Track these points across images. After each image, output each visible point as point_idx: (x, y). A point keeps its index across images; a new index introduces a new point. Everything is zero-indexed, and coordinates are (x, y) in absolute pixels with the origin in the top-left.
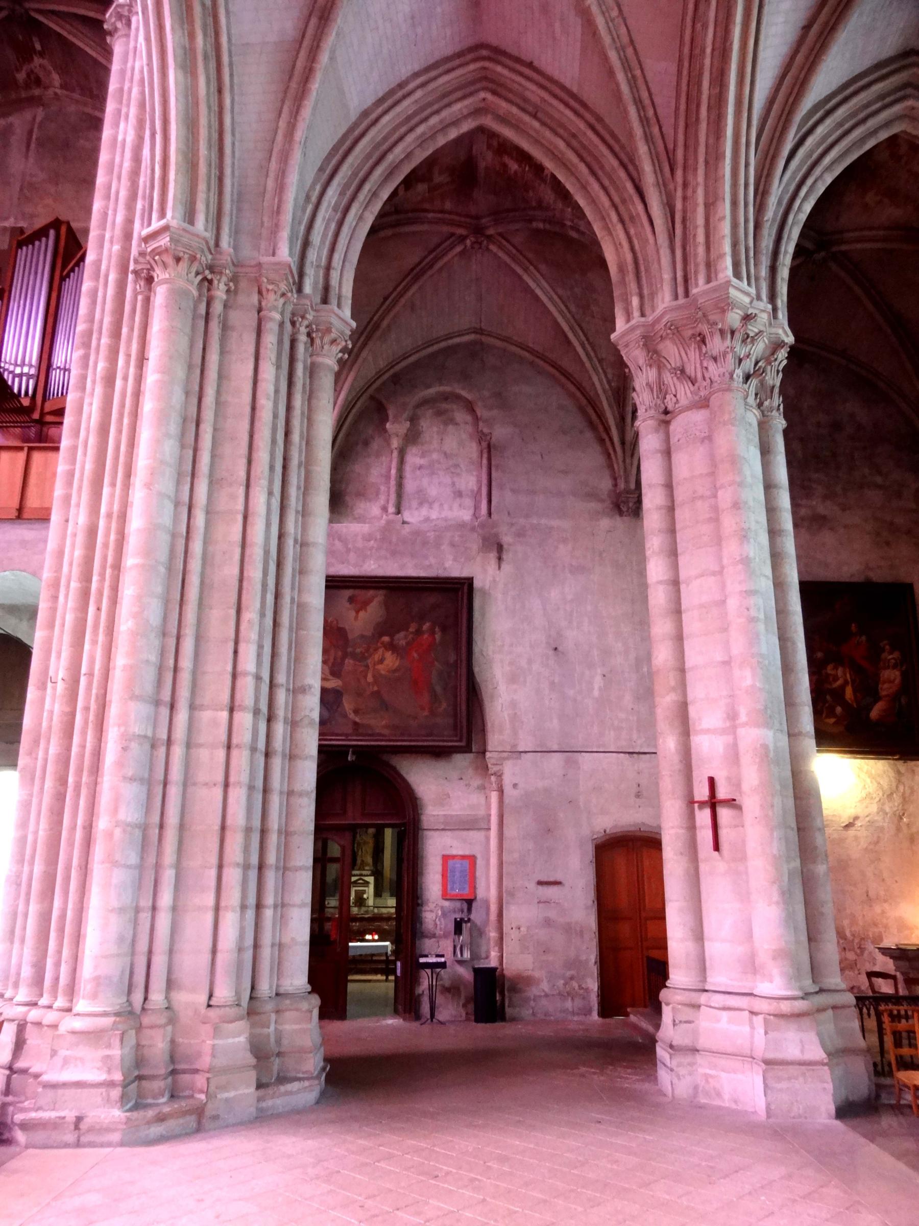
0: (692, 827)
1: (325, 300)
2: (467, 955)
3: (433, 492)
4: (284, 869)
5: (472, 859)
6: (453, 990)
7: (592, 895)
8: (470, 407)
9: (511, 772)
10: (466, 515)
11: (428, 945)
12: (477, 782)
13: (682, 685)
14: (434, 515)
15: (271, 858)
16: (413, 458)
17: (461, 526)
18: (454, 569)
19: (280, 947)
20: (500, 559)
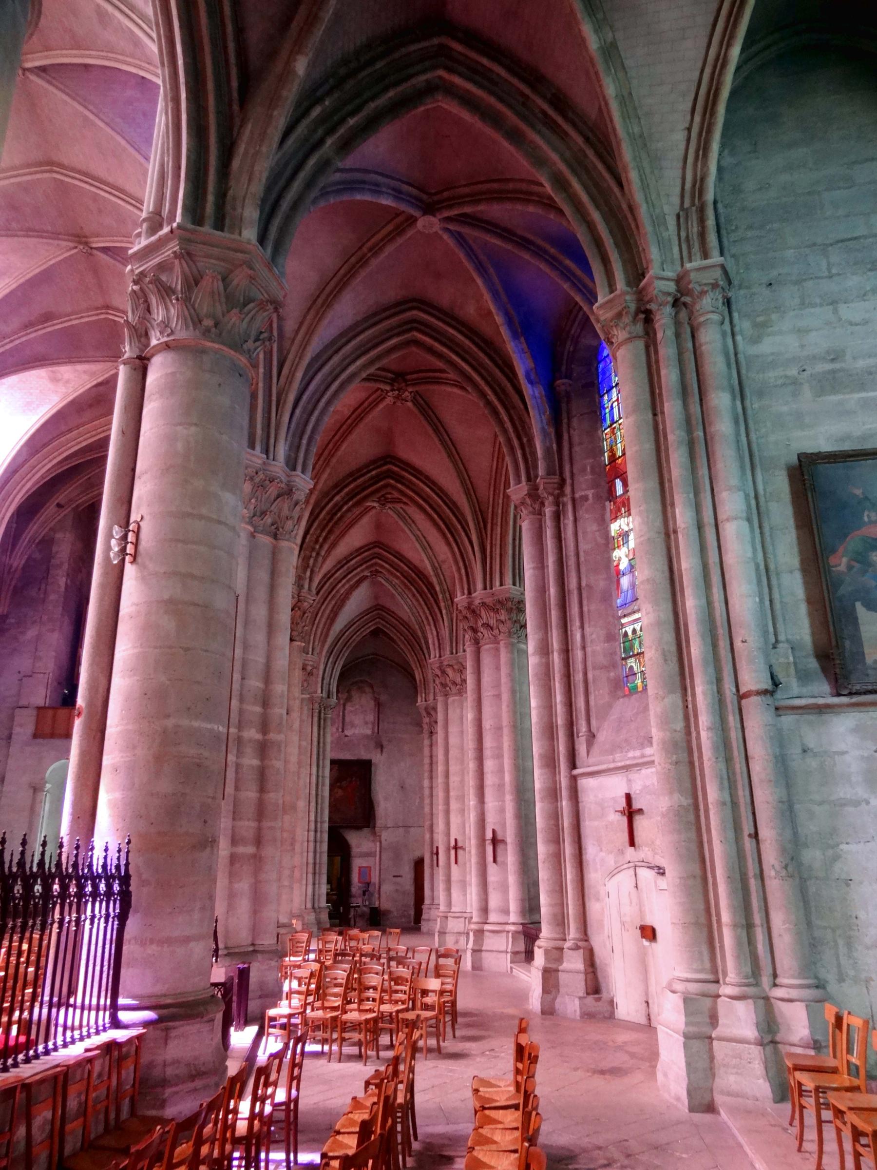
0: (432, 860)
1: (329, 697)
2: (367, 903)
3: (356, 722)
4: (320, 874)
5: (370, 867)
6: (362, 916)
7: (412, 881)
8: (372, 686)
9: (385, 835)
10: (369, 732)
11: (353, 900)
12: (372, 838)
13: (432, 819)
14: (357, 732)
15: (317, 871)
16: (349, 708)
17: (367, 736)
18: (364, 755)
19: (319, 895)
20: (382, 751)
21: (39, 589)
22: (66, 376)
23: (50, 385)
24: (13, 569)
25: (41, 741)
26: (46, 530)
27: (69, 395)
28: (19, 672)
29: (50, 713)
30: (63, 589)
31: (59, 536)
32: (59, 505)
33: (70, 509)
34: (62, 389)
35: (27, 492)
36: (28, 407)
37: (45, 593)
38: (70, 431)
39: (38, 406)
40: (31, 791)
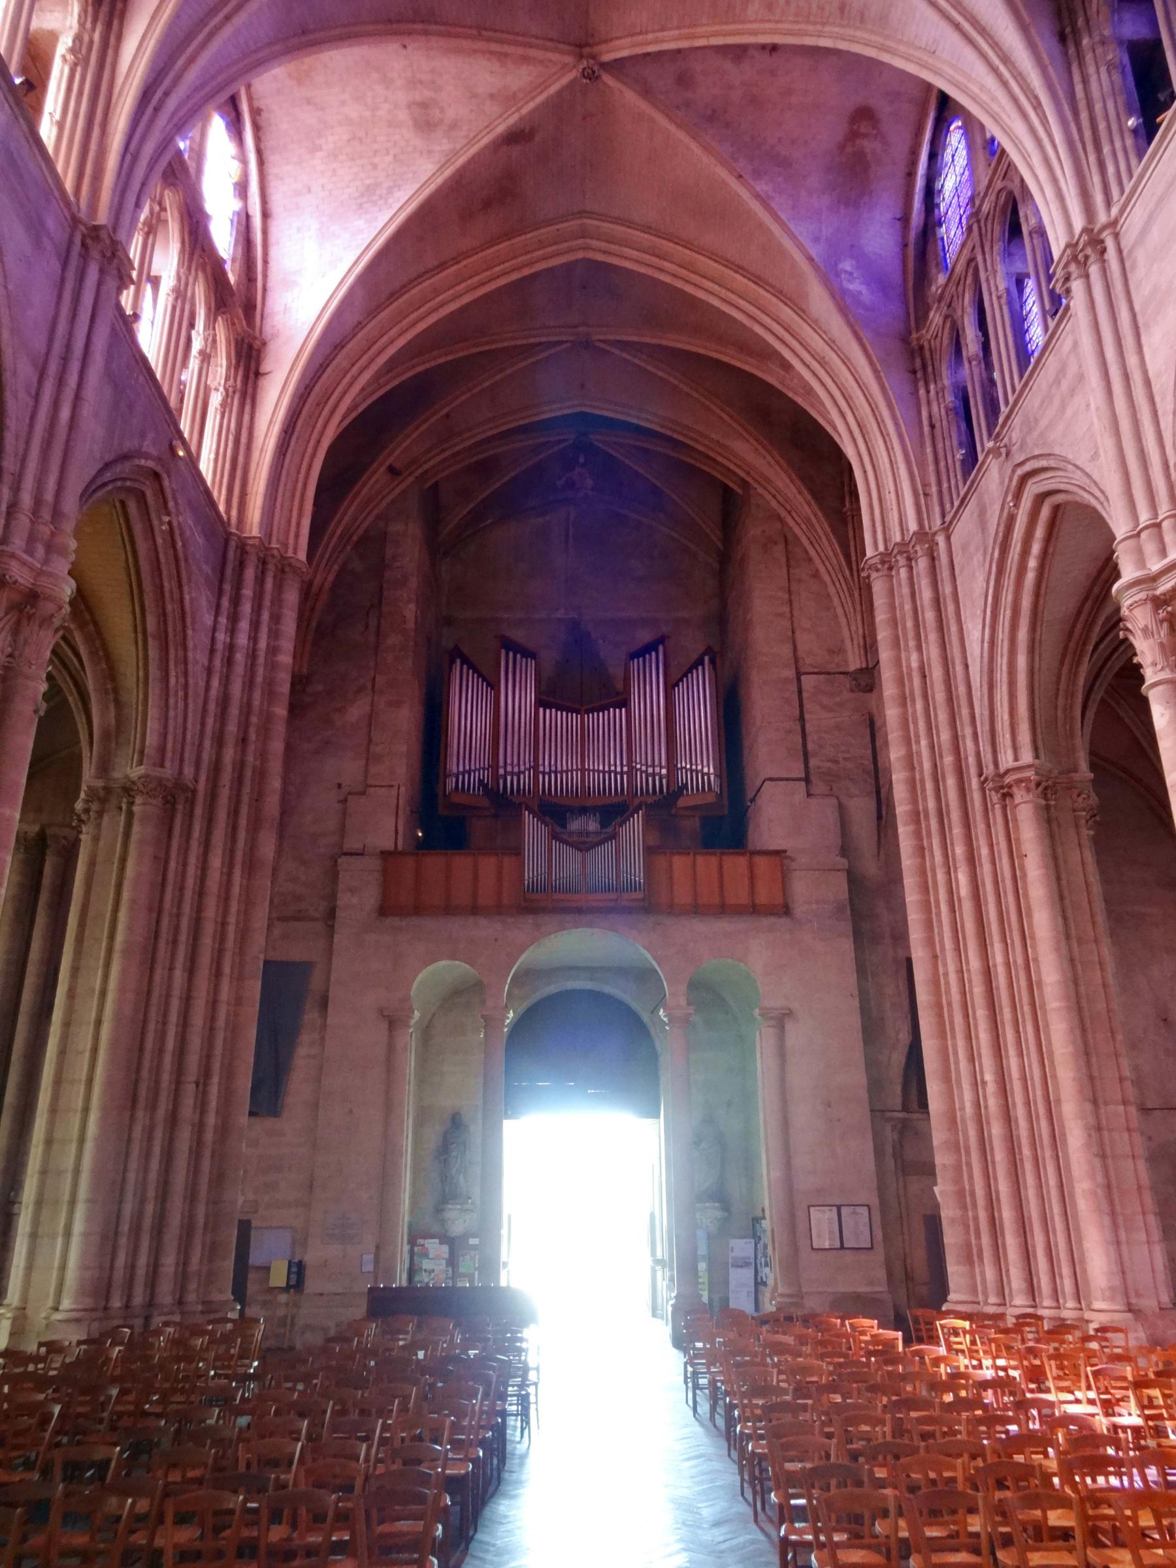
21: (367, 627)
22: (451, 113)
23: (417, 142)
24: (314, 590)
25: (395, 921)
26: (371, 518)
27: (456, 153)
28: (339, 786)
29: (410, 862)
30: (411, 625)
31: (396, 527)
32: (393, 471)
33: (411, 479)
34: (443, 145)
35: (350, 410)
36: (369, 195)
37: (378, 633)
38: (442, 266)
39: (390, 191)
40: (384, 1025)
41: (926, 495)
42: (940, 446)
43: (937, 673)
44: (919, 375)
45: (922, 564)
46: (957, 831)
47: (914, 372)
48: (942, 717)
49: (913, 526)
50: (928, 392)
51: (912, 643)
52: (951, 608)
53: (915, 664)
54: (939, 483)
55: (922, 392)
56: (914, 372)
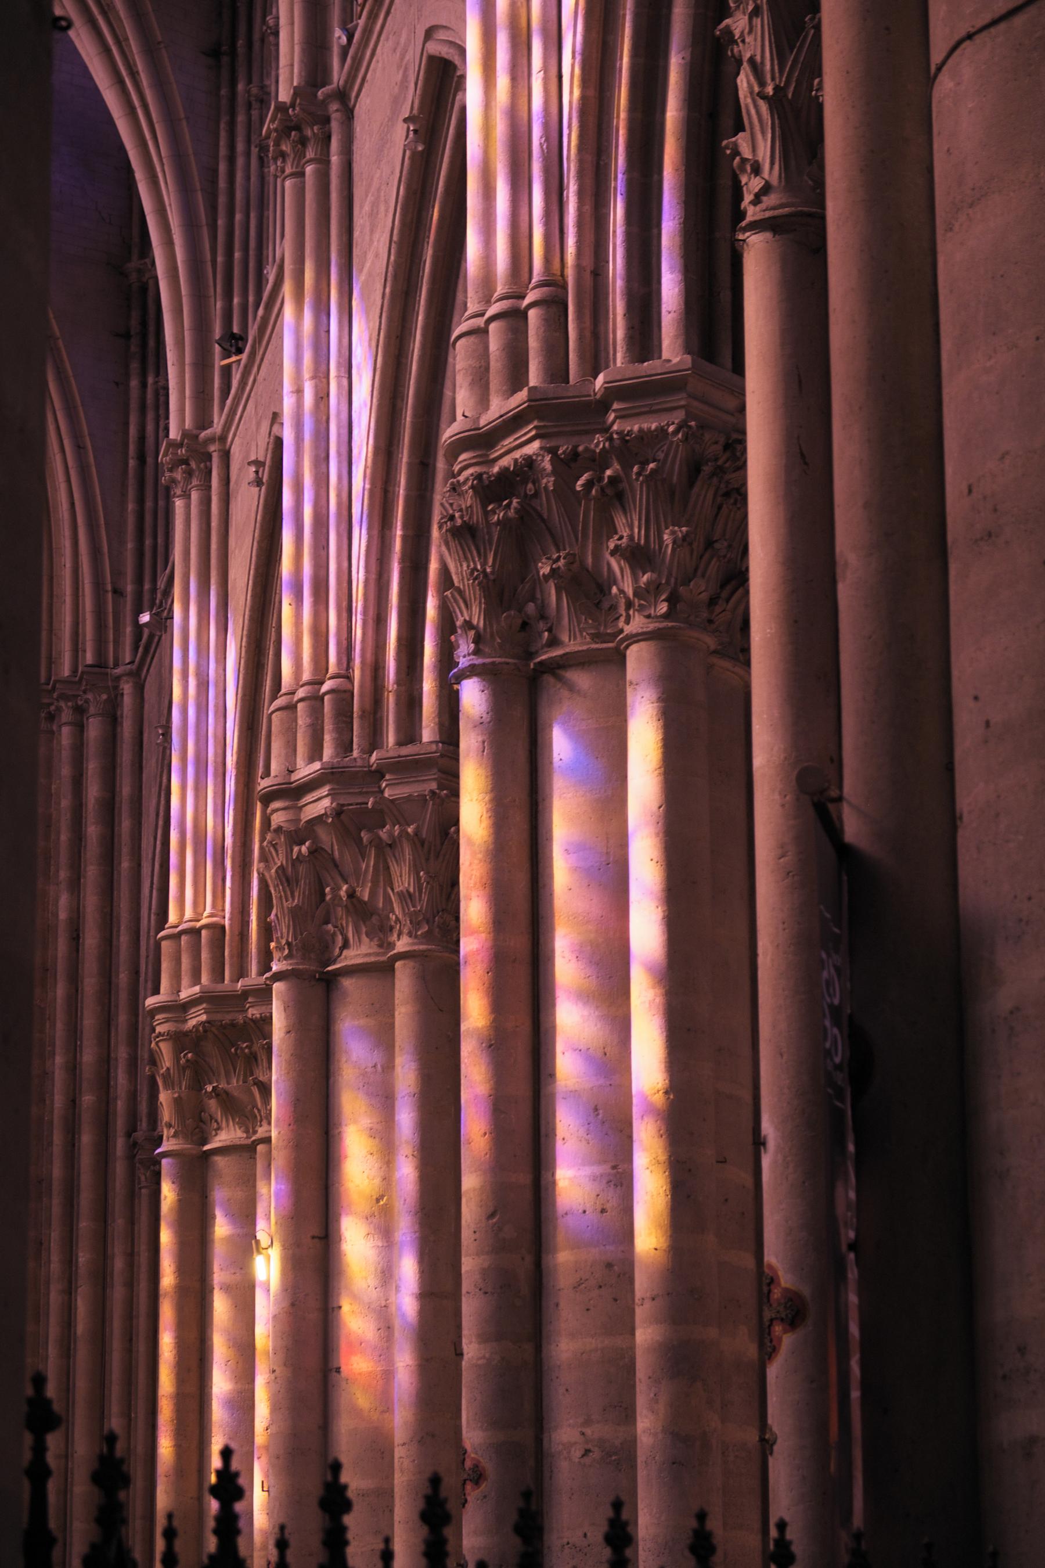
41: (115, 591)
42: (149, 504)
43: (91, 940)
44: (134, 348)
45: (94, 729)
46: (85, 1225)
47: (127, 336)
48: (89, 1022)
49: (89, 658)
50: (144, 385)
51: (63, 874)
52: (125, 825)
53: (63, 915)
54: (139, 580)
55: (134, 383)
56: (127, 336)
